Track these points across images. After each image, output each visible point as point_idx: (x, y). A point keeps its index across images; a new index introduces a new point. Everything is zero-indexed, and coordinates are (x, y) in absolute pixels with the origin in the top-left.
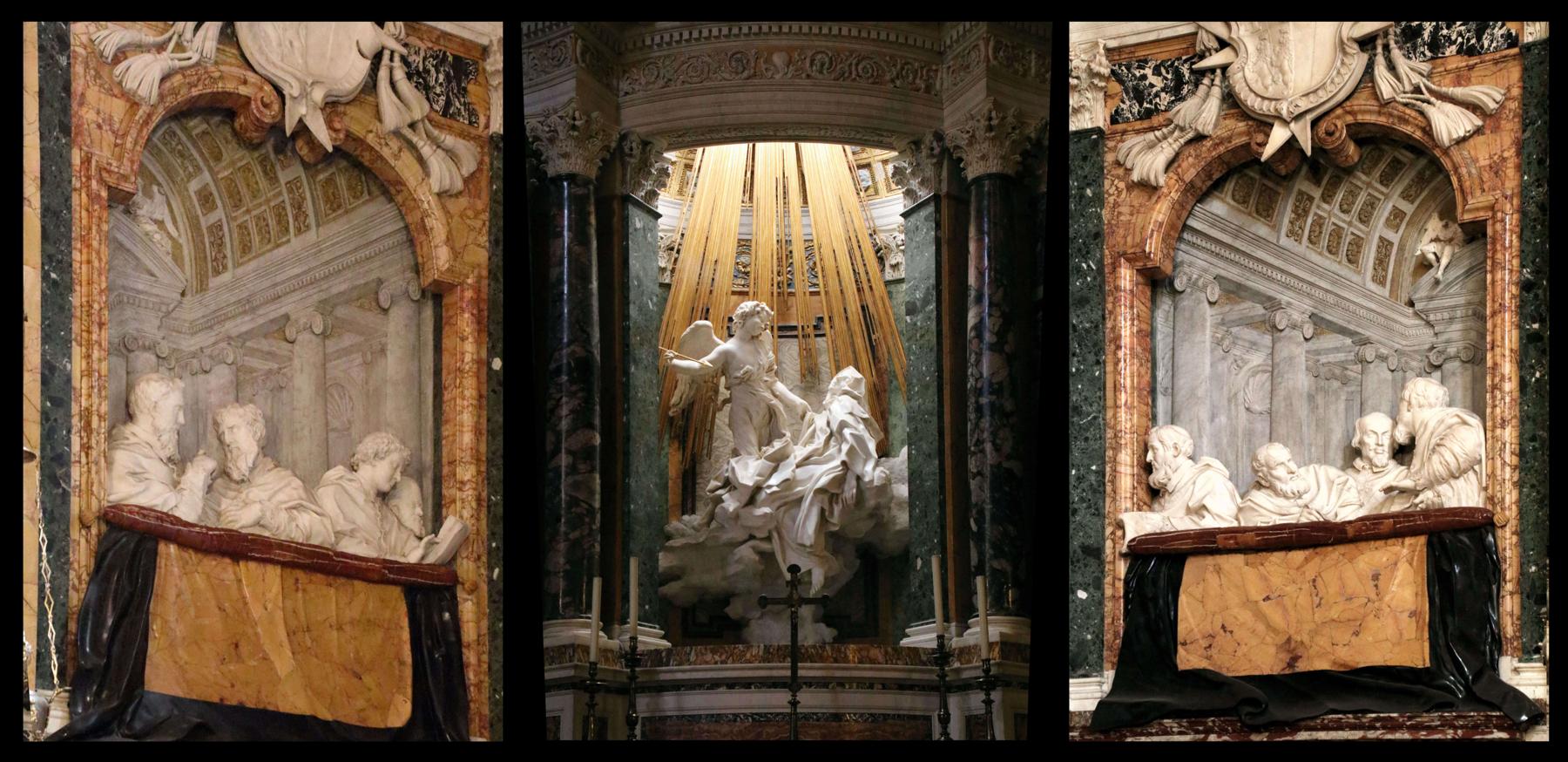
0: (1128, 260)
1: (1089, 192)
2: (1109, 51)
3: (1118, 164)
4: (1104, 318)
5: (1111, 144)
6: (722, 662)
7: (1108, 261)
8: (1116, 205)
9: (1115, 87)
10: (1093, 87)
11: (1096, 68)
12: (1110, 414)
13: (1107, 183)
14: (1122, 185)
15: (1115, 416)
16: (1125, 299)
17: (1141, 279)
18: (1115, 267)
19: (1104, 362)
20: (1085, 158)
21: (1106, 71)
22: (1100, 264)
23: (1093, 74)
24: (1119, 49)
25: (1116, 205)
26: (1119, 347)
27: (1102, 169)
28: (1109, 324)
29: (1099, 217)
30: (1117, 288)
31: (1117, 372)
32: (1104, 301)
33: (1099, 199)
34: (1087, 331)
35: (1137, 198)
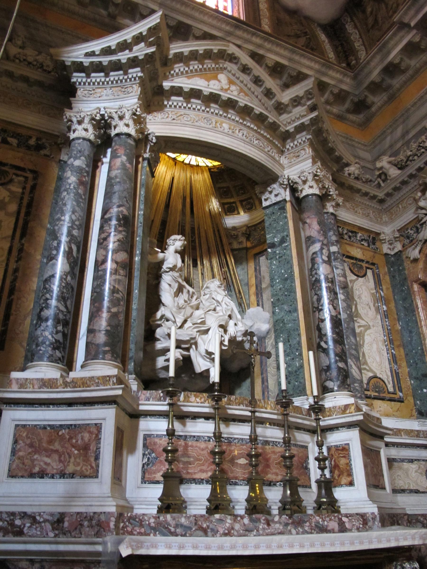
0: (415, 282)
1: (401, 268)
2: (398, 231)
3: (407, 257)
4: (412, 301)
5: (404, 253)
6: (201, 403)
7: (410, 285)
8: (409, 268)
9: (402, 238)
10: (396, 241)
11: (396, 236)
12: (420, 330)
13: (405, 264)
14: (409, 262)
15: (422, 330)
16: (417, 293)
17: (420, 286)
18: (412, 285)
19: (415, 315)
20: (398, 260)
21: (398, 236)
22: (408, 287)
23: (395, 238)
24: (401, 229)
25: (409, 268)
26: (418, 308)
27: (403, 260)
28: (414, 303)
29: (405, 274)
30: (414, 291)
31: (419, 316)
32: (411, 296)
33: (404, 269)
34: (409, 307)
35: (413, 265)
